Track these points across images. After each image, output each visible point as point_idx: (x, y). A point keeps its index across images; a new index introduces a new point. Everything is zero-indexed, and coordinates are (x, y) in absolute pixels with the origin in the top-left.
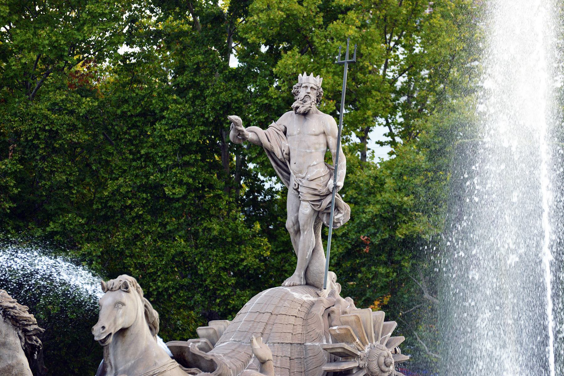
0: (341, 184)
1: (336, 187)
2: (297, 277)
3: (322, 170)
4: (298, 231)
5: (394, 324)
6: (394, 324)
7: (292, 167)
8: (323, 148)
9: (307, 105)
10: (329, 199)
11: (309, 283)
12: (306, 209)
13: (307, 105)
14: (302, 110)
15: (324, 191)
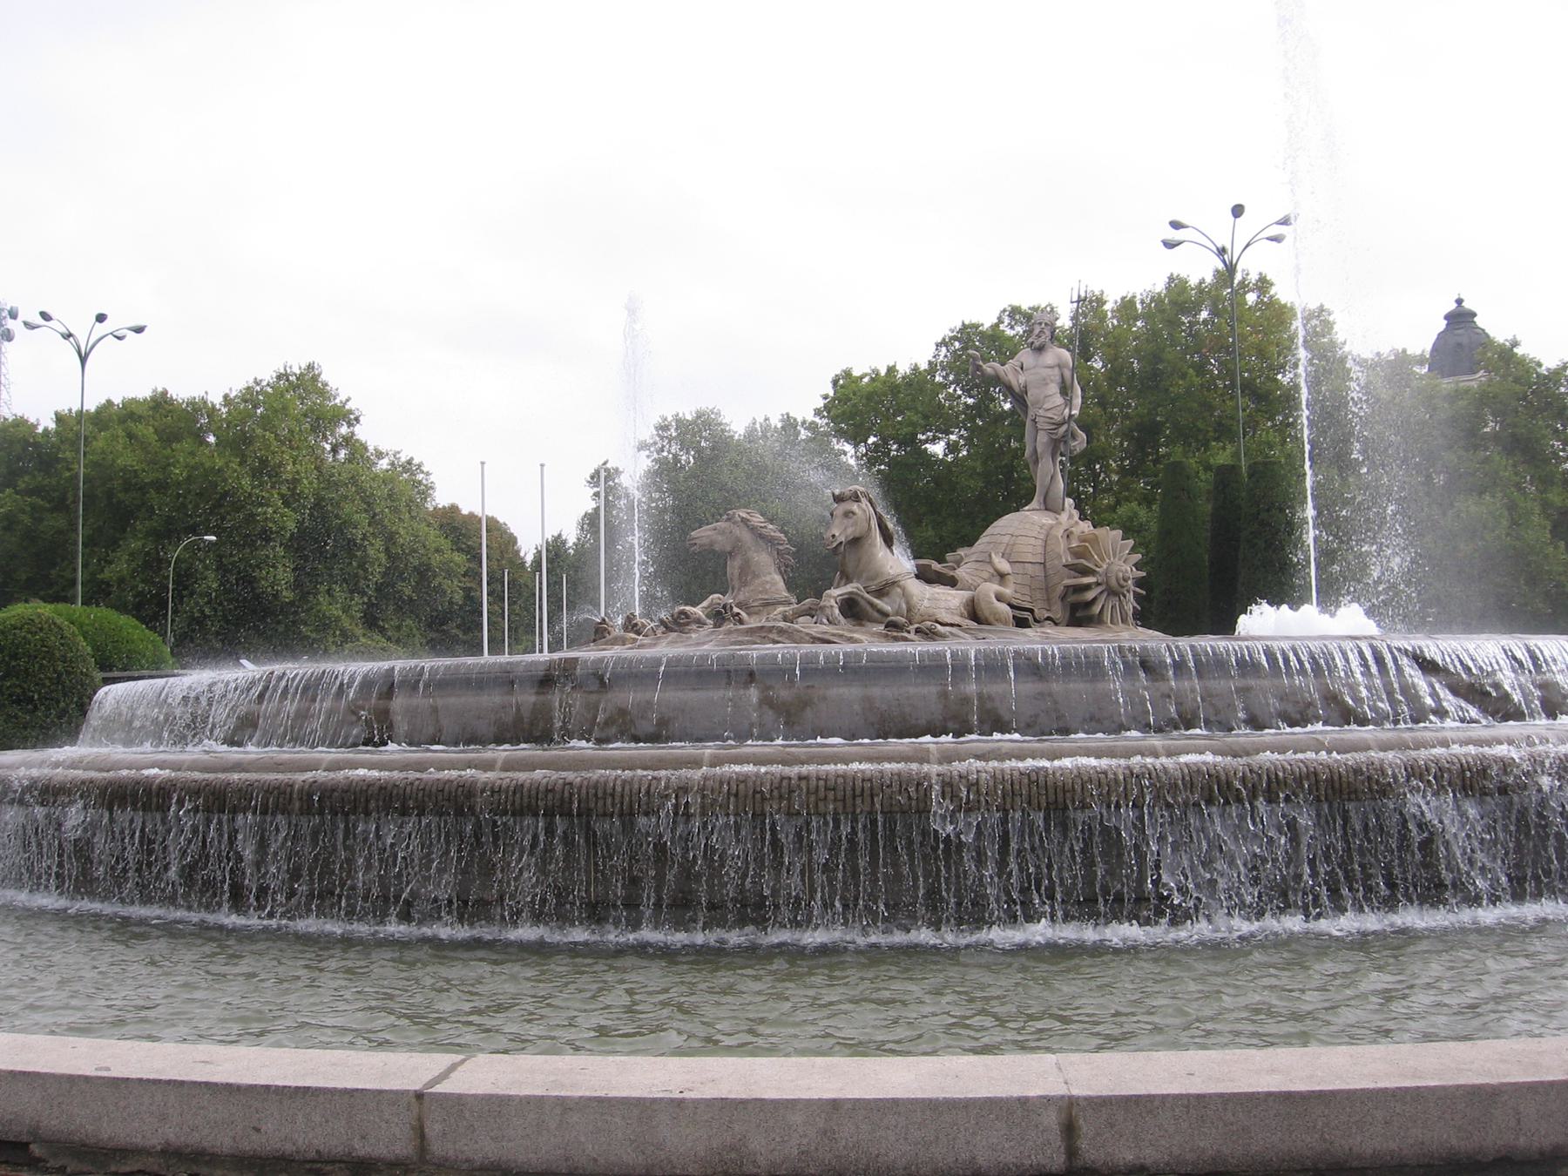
0: (1075, 412)
1: (1071, 416)
2: (1034, 504)
3: (1059, 400)
4: (1036, 462)
5: (1131, 542)
6: (1131, 542)
7: (1030, 399)
8: (1058, 378)
9: (1042, 339)
10: (1064, 427)
11: (1049, 507)
12: (1042, 438)
13: (1042, 339)
14: (1037, 344)
15: (1058, 419)
